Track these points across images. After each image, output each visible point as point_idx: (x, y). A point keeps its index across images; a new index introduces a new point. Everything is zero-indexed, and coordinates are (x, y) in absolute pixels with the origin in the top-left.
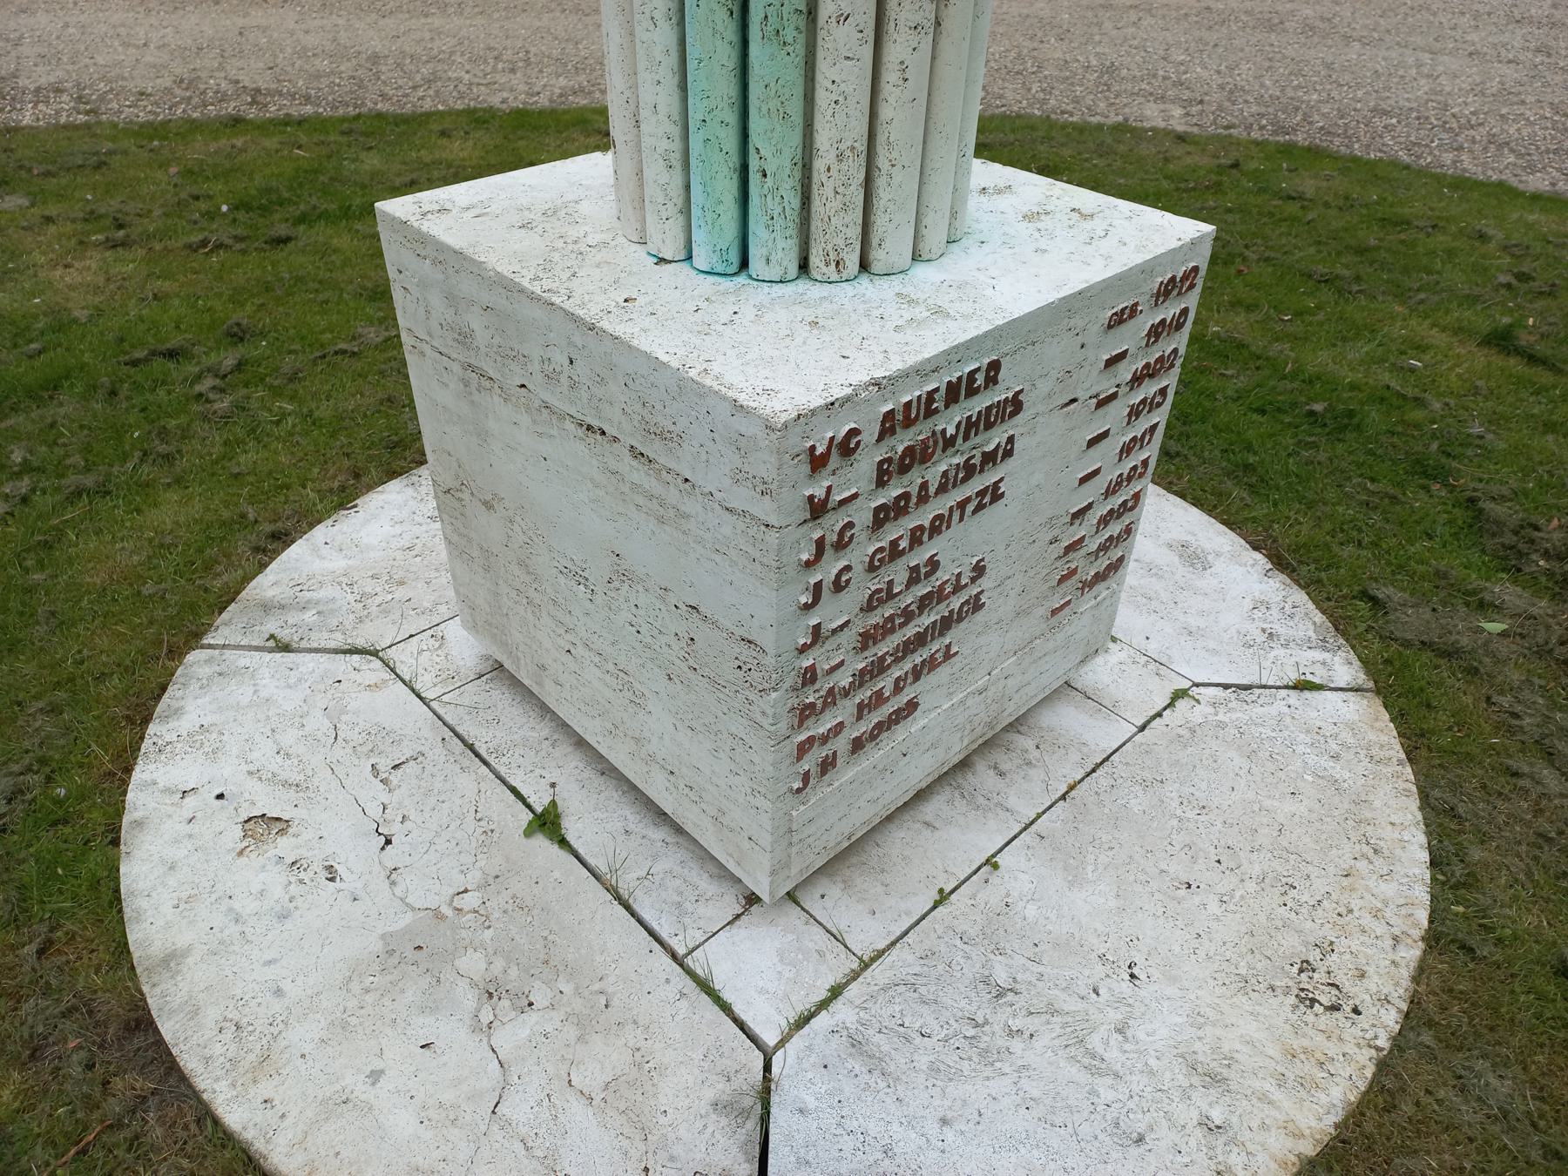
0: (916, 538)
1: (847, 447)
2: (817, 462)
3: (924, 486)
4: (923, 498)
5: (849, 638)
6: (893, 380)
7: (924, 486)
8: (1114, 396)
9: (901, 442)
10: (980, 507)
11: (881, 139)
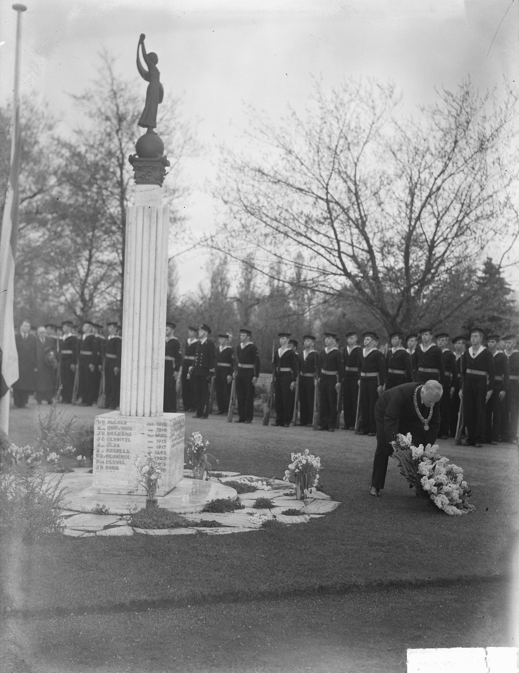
0: (115, 439)
5: (105, 448)
8: (152, 436)
10: (126, 441)
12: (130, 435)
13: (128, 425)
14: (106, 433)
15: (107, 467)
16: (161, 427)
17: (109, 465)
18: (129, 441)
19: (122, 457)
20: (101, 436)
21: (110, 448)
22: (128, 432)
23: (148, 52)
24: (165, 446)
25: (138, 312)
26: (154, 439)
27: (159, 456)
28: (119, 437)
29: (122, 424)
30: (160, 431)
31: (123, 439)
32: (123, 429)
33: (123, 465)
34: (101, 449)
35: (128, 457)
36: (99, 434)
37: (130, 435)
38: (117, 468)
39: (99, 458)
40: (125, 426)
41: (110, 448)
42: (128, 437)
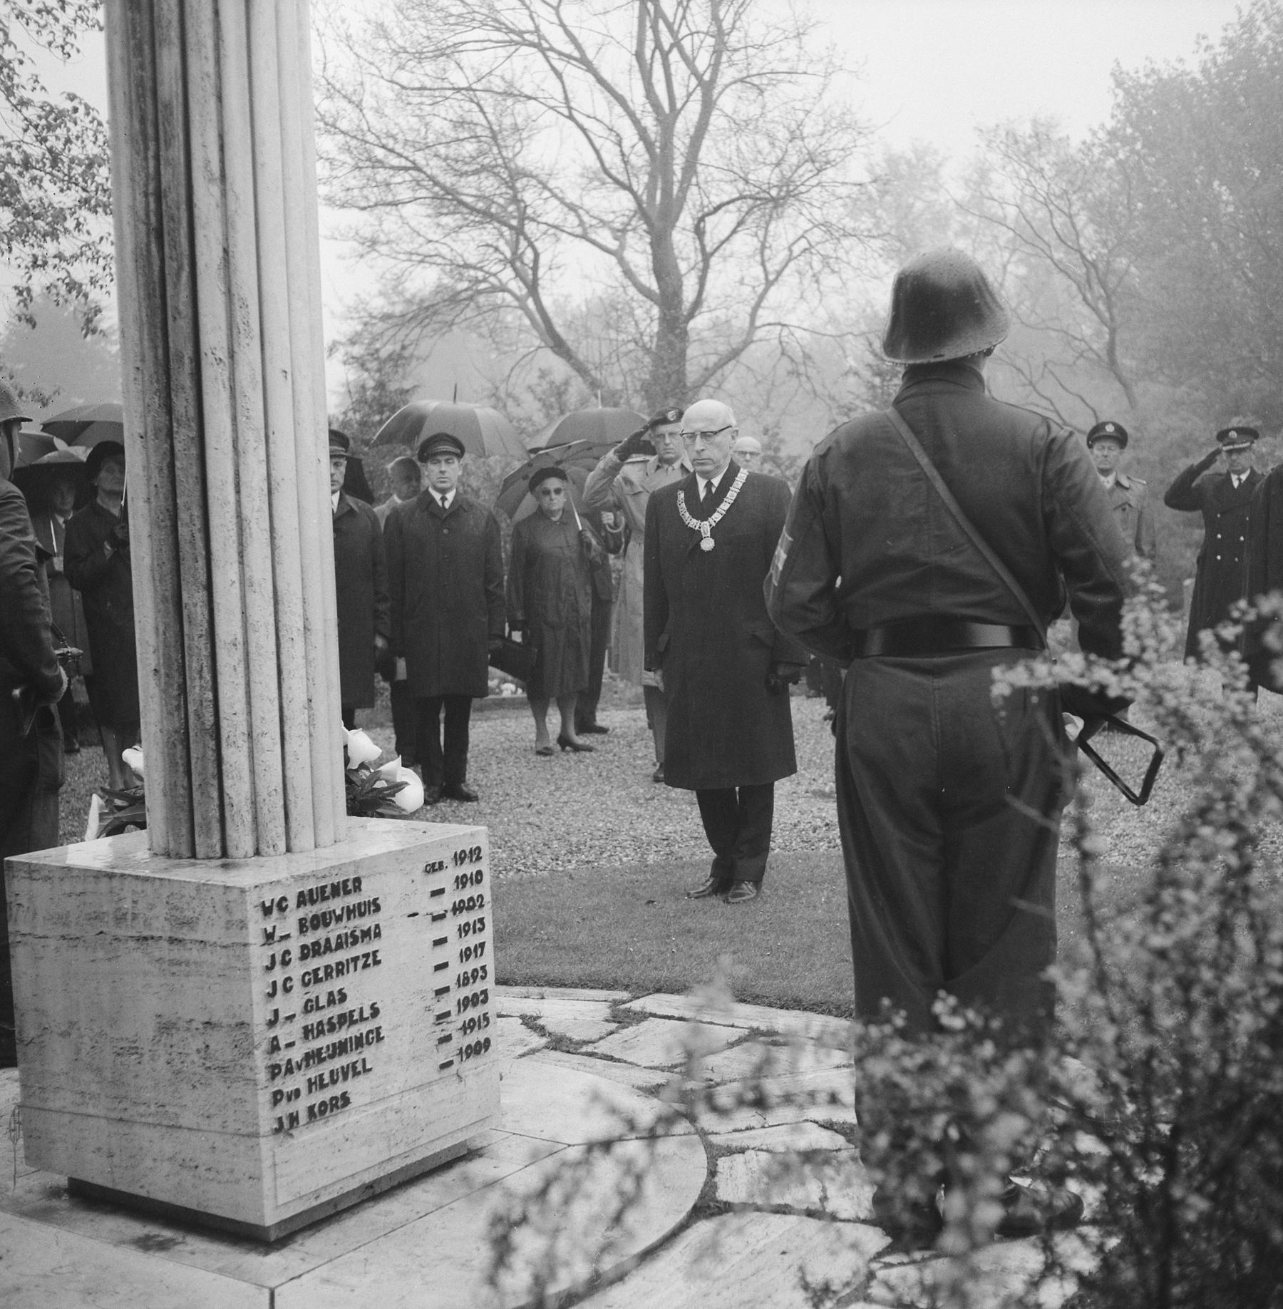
1: (282, 905)
2: (267, 911)
3: (328, 940)
4: (328, 948)
6: (302, 877)
7: (328, 940)
8: (442, 917)
9: (309, 911)
10: (365, 966)
11: (289, 787)
13: (366, 894)
14: (295, 954)
18: (377, 962)
19: (359, 1042)
20: (278, 975)
21: (314, 1018)
22: (367, 922)
24: (482, 945)
26: (449, 928)
28: (342, 955)
29: (347, 892)
30: (464, 886)
31: (355, 959)
32: (350, 912)
33: (361, 1078)
34: (284, 1033)
35: (378, 1036)
40: (352, 900)
41: (314, 1018)
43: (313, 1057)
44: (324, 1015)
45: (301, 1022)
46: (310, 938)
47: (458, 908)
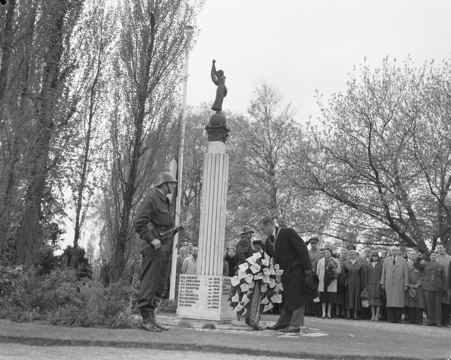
0: (190, 288)
5: (184, 294)
9: (188, 279)
12: (199, 285)
13: (198, 279)
15: (185, 305)
16: (217, 281)
17: (186, 303)
19: (194, 299)
21: (187, 293)
22: (198, 283)
23: (217, 70)
25: (207, 213)
26: (212, 288)
27: (215, 298)
28: (193, 286)
32: (195, 281)
34: (182, 293)
36: (182, 285)
37: (199, 285)
38: (191, 306)
39: (181, 299)
41: (187, 293)
42: (198, 287)
43: (187, 298)
44: (189, 293)
45: (185, 293)
46: (188, 283)
47: (214, 286)
